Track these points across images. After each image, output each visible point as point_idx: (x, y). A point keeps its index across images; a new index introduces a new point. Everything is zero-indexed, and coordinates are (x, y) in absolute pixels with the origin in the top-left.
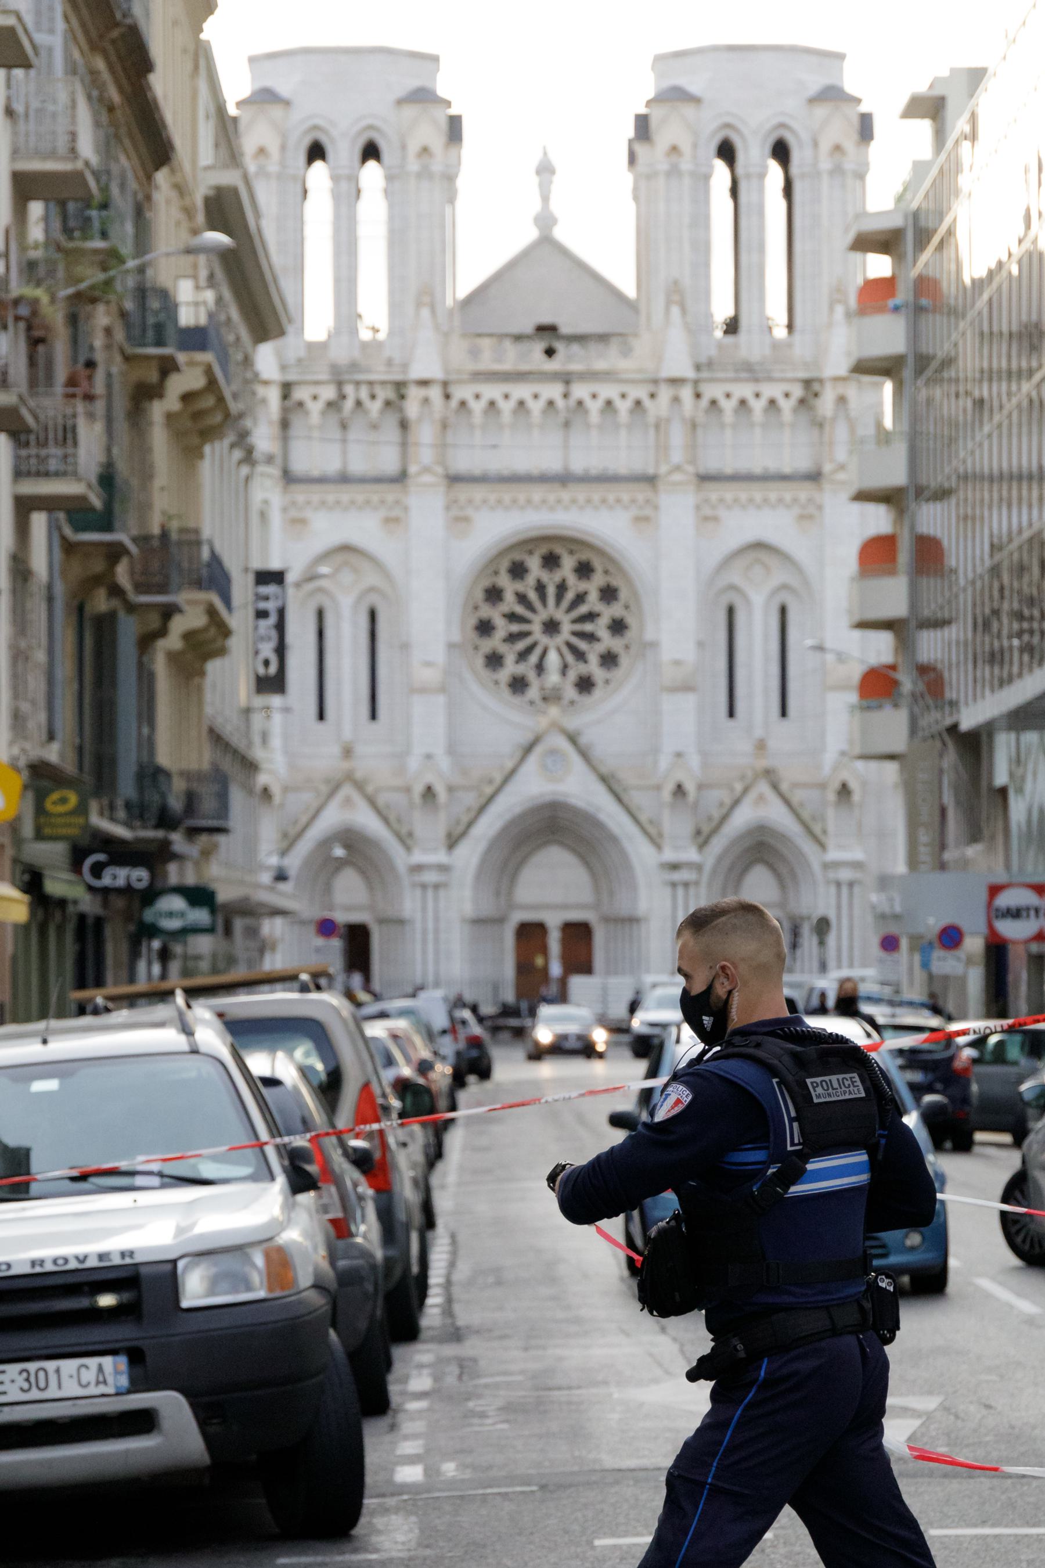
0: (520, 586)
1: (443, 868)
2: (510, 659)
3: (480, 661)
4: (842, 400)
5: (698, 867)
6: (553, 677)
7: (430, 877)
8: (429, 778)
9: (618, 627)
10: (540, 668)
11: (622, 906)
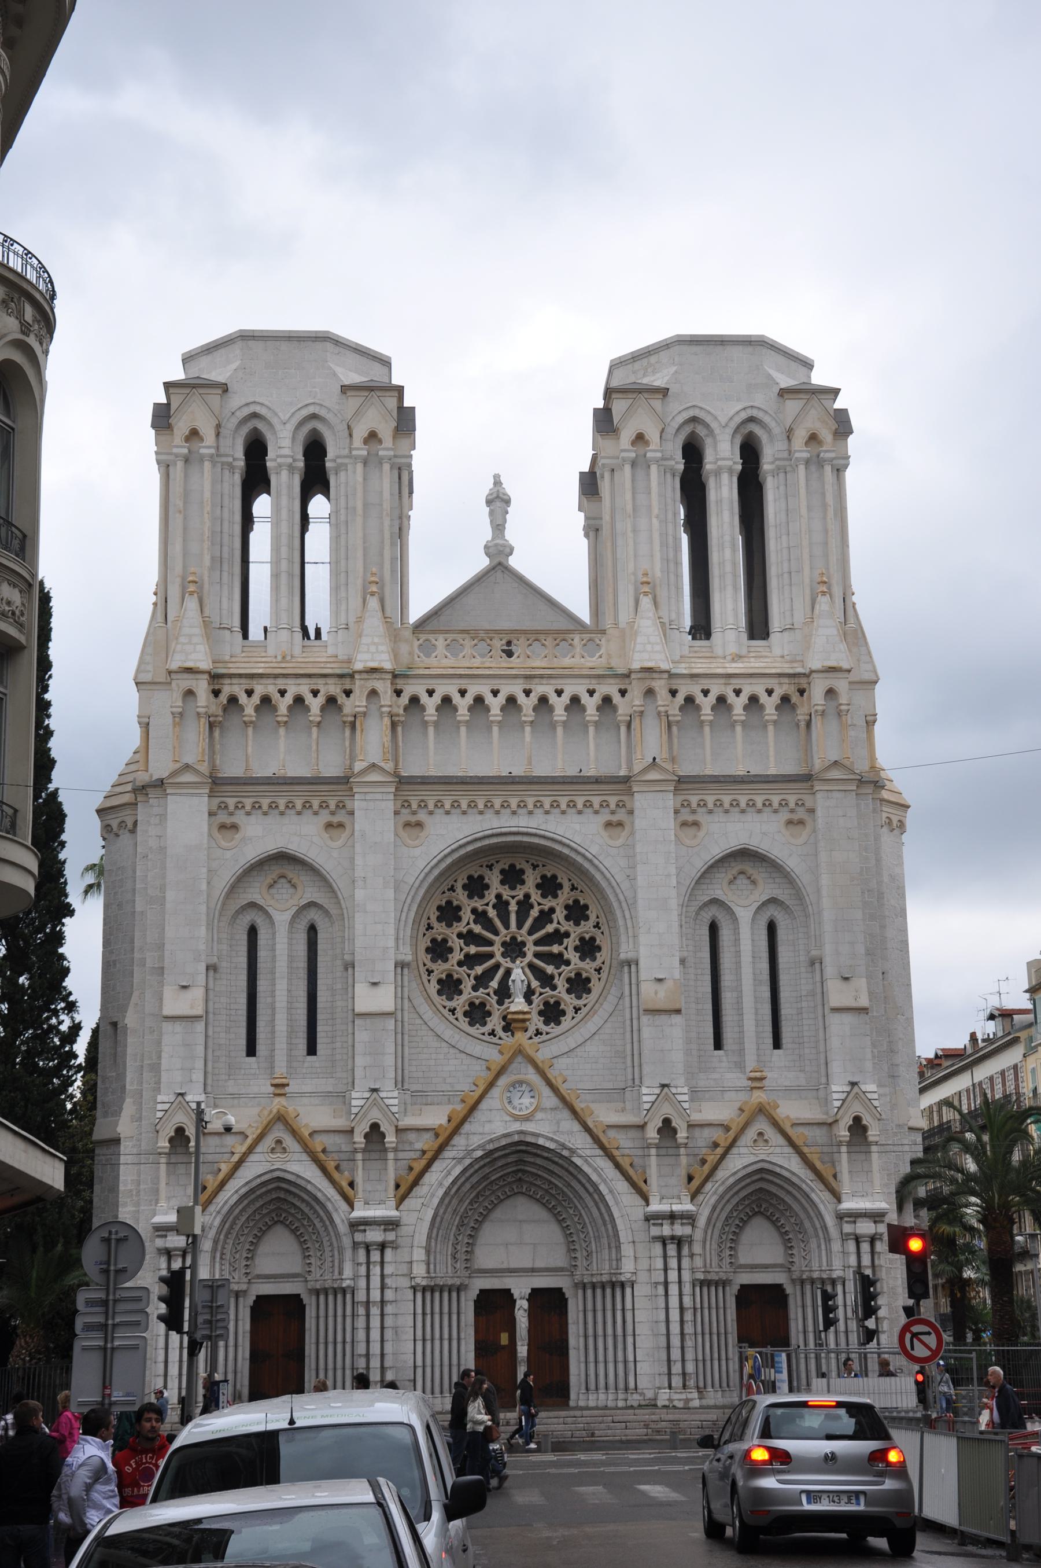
0: (478, 904)
1: (391, 1225)
2: (468, 984)
3: (433, 987)
4: (830, 692)
5: (689, 1218)
6: (518, 1004)
7: (374, 1235)
8: (375, 1116)
9: (588, 948)
10: (504, 993)
11: (601, 1269)
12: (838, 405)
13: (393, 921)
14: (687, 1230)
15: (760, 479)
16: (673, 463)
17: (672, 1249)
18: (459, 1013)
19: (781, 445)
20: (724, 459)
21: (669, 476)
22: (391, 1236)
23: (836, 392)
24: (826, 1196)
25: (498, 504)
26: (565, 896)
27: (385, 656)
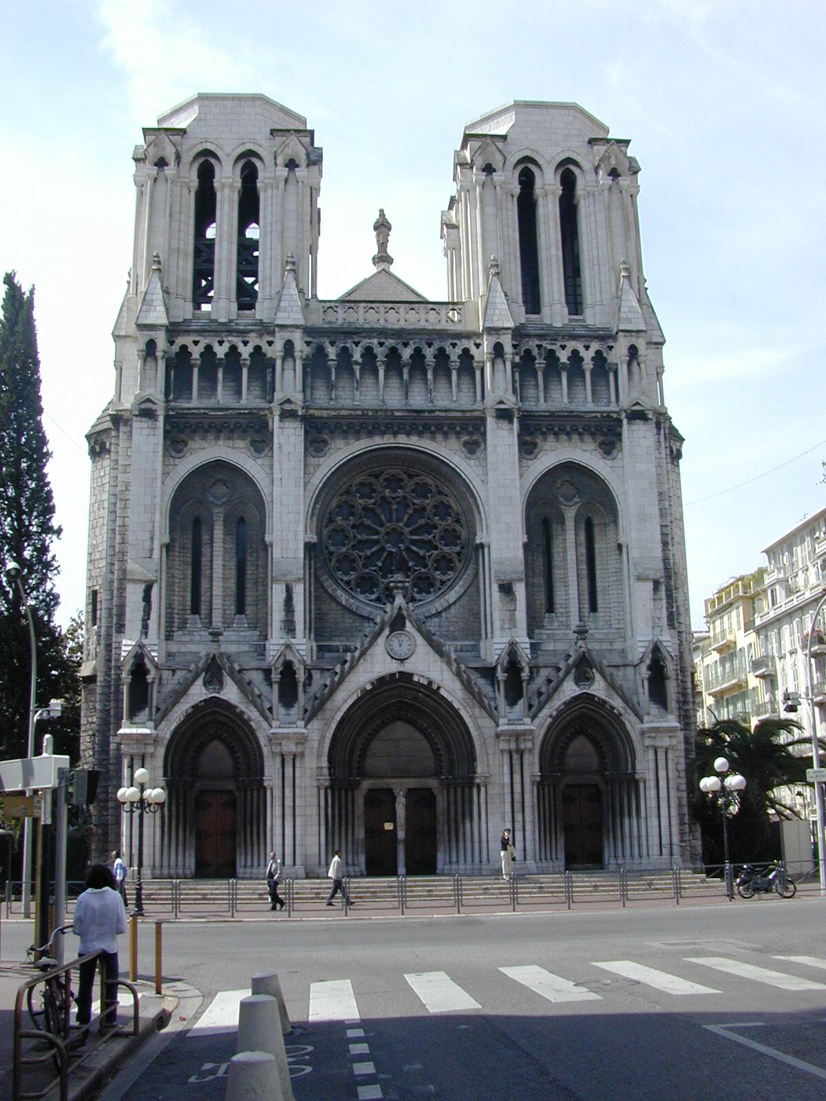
1: (302, 740)
13: (302, 512)
14: (529, 745)
15: (575, 202)
16: (512, 186)
17: (516, 757)
19: (590, 177)
20: (548, 185)
21: (510, 197)
22: (300, 748)
23: (627, 142)
24: (634, 718)
25: (383, 229)
27: (300, 316)
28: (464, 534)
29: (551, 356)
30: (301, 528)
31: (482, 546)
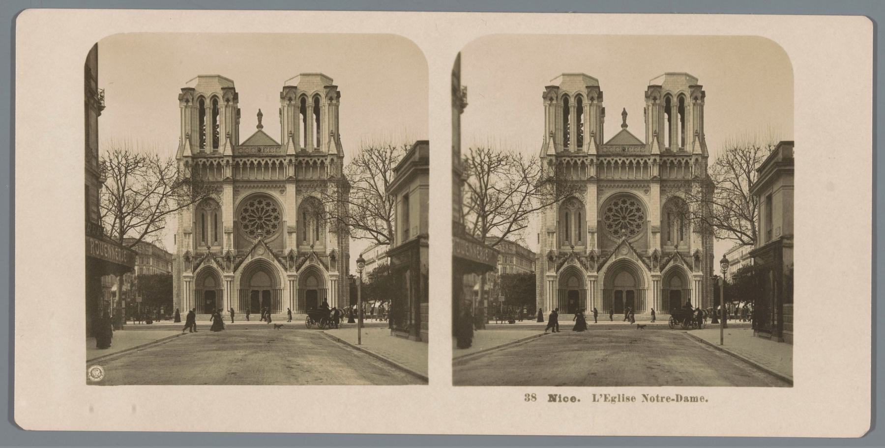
12: (338, 90)
18: (248, 232)
26: (271, 207)
28: (280, 218)
29: (307, 163)
30: (232, 217)
31: (284, 221)
